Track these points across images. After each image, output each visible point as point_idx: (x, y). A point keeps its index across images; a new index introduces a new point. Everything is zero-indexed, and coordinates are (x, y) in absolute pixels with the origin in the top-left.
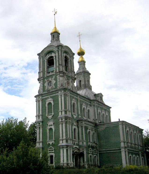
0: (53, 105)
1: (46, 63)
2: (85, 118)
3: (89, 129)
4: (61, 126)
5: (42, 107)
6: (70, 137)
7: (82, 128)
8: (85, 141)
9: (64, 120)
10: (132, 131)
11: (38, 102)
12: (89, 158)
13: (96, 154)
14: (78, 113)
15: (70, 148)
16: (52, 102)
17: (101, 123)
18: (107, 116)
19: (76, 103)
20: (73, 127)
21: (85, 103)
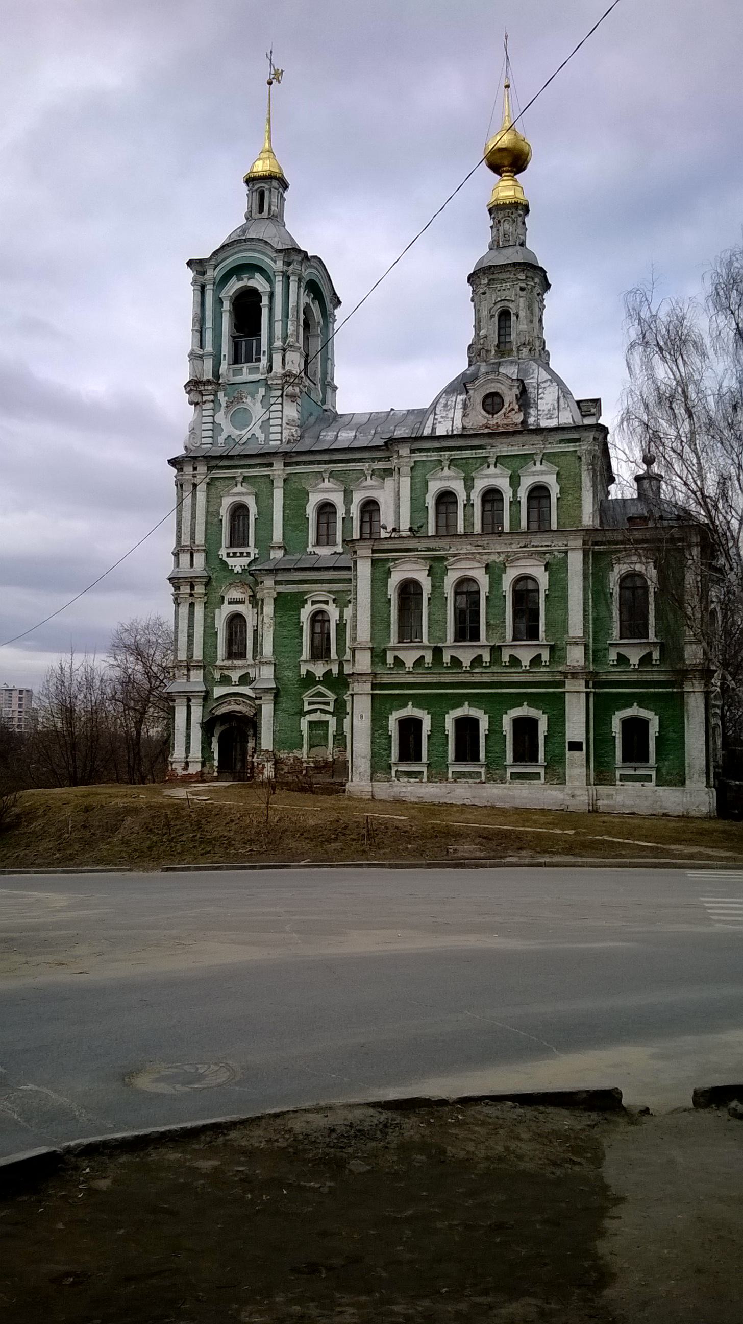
19: (250, 502)
20: (217, 611)
21: (332, 475)
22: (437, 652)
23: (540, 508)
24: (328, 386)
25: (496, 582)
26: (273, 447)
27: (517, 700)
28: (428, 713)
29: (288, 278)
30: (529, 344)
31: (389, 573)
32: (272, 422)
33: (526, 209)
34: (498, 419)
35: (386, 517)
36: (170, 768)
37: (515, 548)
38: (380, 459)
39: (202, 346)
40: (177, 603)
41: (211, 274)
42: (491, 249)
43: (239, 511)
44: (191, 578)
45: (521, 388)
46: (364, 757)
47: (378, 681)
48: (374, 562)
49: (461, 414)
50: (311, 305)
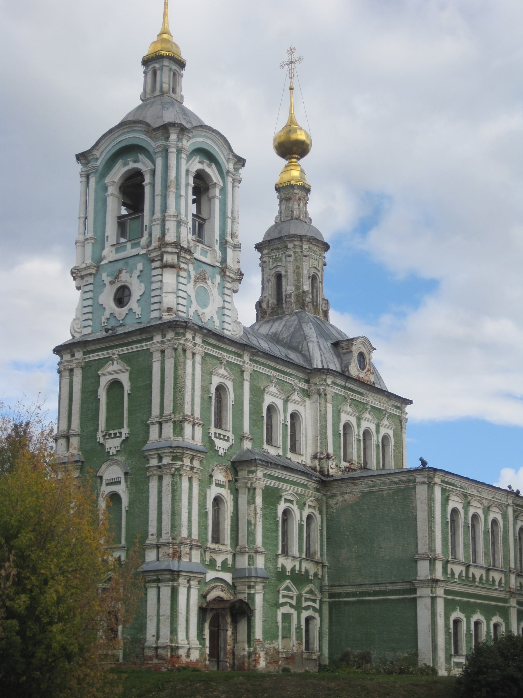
0: (129, 394)
1: (110, 200)
2: (273, 451)
3: (287, 500)
4: (153, 485)
5: (83, 401)
6: (190, 534)
7: (254, 493)
8: (262, 553)
9: (166, 460)
10: (480, 512)
11: (66, 374)
12: (277, 623)
13: (317, 606)
14: (237, 428)
15: (189, 581)
16: (125, 379)
17: (348, 469)
18: (385, 438)
34: (362, 375)
37: (490, 497)
48: (443, 490)
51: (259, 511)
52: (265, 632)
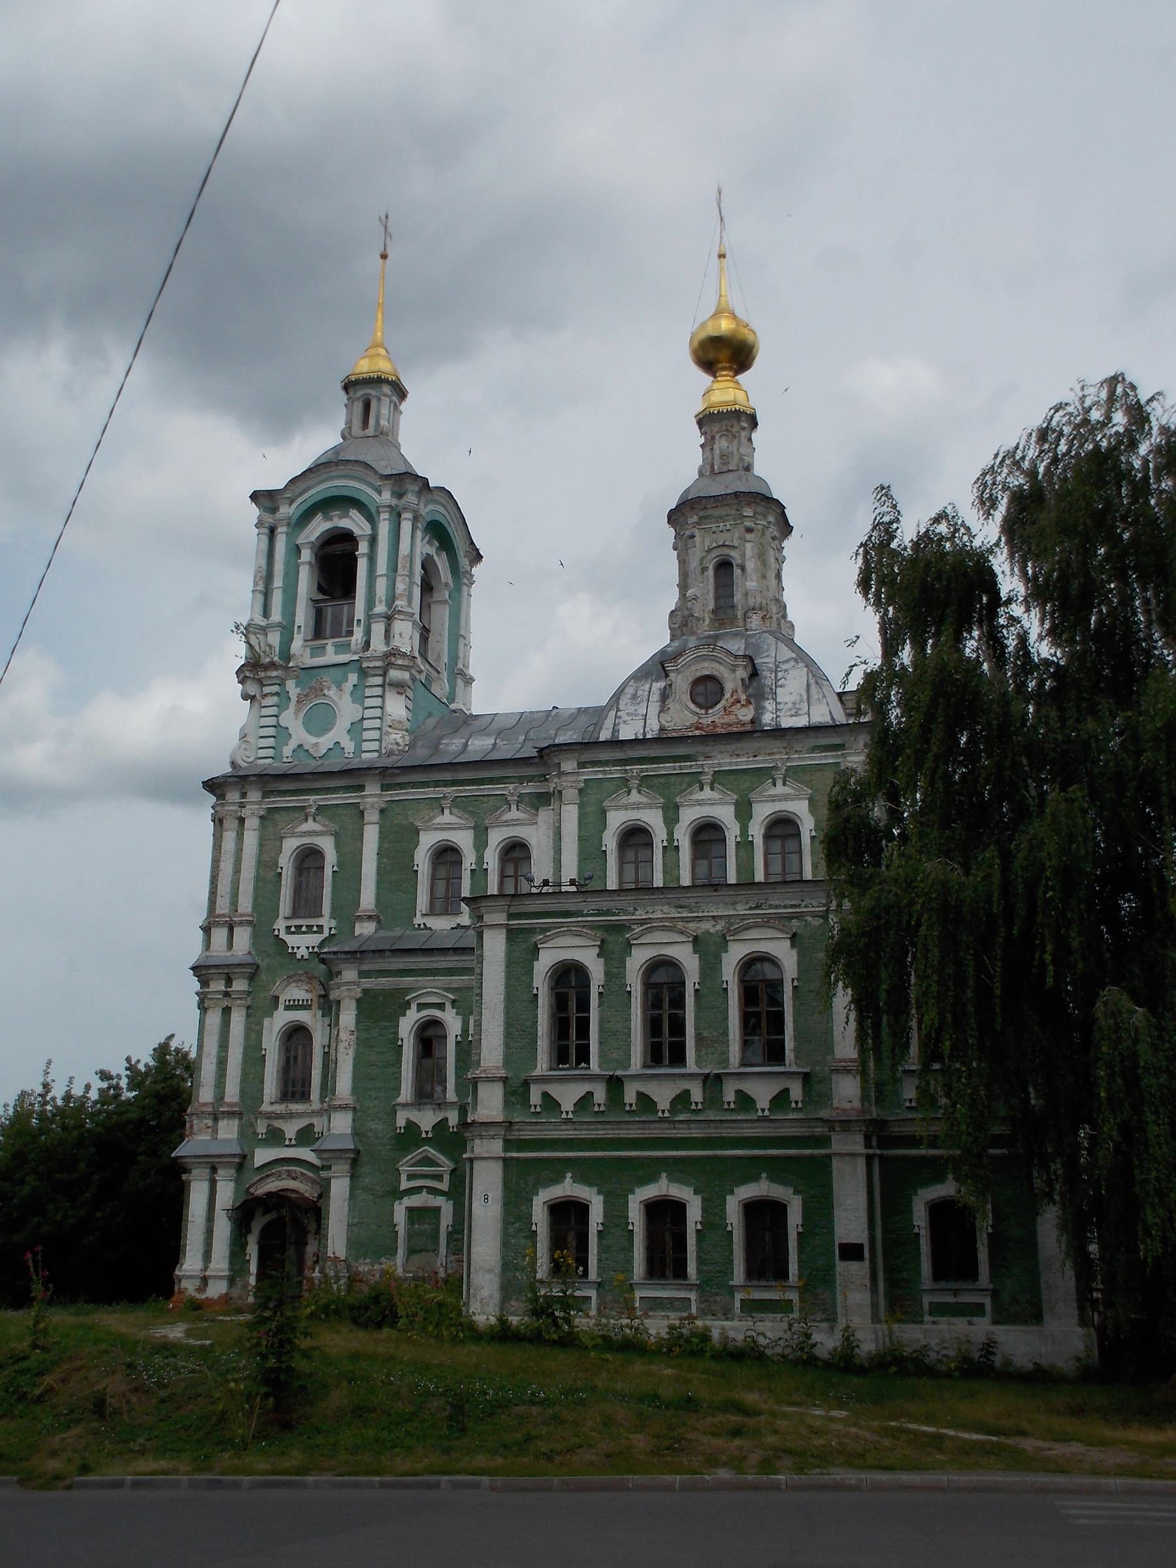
6: (220, 1097)
19: (327, 845)
20: (266, 1022)
21: (457, 803)
22: (615, 1084)
23: (784, 854)
24: (461, 676)
25: (710, 967)
26: (366, 761)
27: (748, 1170)
28: (599, 1193)
29: (399, 515)
30: (760, 609)
31: (535, 951)
32: (367, 724)
33: (754, 423)
34: (715, 716)
35: (540, 868)
36: (176, 1287)
37: (741, 910)
38: (531, 779)
39: (266, 613)
40: (203, 1007)
41: (286, 511)
42: (701, 474)
43: (309, 858)
44: (227, 966)
45: (750, 669)
46: (489, 1271)
47: (515, 1135)
48: (513, 934)
49: (657, 709)
50: (436, 557)
51: (343, 1035)
52: (351, 1243)
